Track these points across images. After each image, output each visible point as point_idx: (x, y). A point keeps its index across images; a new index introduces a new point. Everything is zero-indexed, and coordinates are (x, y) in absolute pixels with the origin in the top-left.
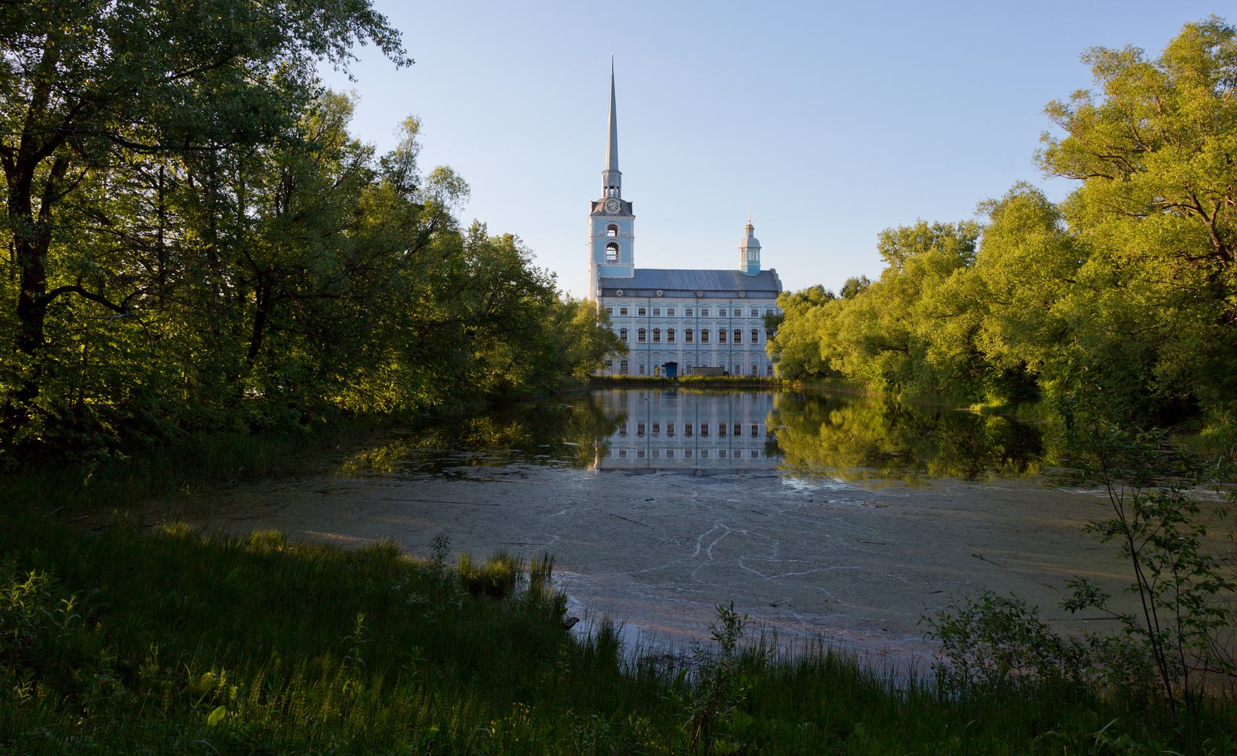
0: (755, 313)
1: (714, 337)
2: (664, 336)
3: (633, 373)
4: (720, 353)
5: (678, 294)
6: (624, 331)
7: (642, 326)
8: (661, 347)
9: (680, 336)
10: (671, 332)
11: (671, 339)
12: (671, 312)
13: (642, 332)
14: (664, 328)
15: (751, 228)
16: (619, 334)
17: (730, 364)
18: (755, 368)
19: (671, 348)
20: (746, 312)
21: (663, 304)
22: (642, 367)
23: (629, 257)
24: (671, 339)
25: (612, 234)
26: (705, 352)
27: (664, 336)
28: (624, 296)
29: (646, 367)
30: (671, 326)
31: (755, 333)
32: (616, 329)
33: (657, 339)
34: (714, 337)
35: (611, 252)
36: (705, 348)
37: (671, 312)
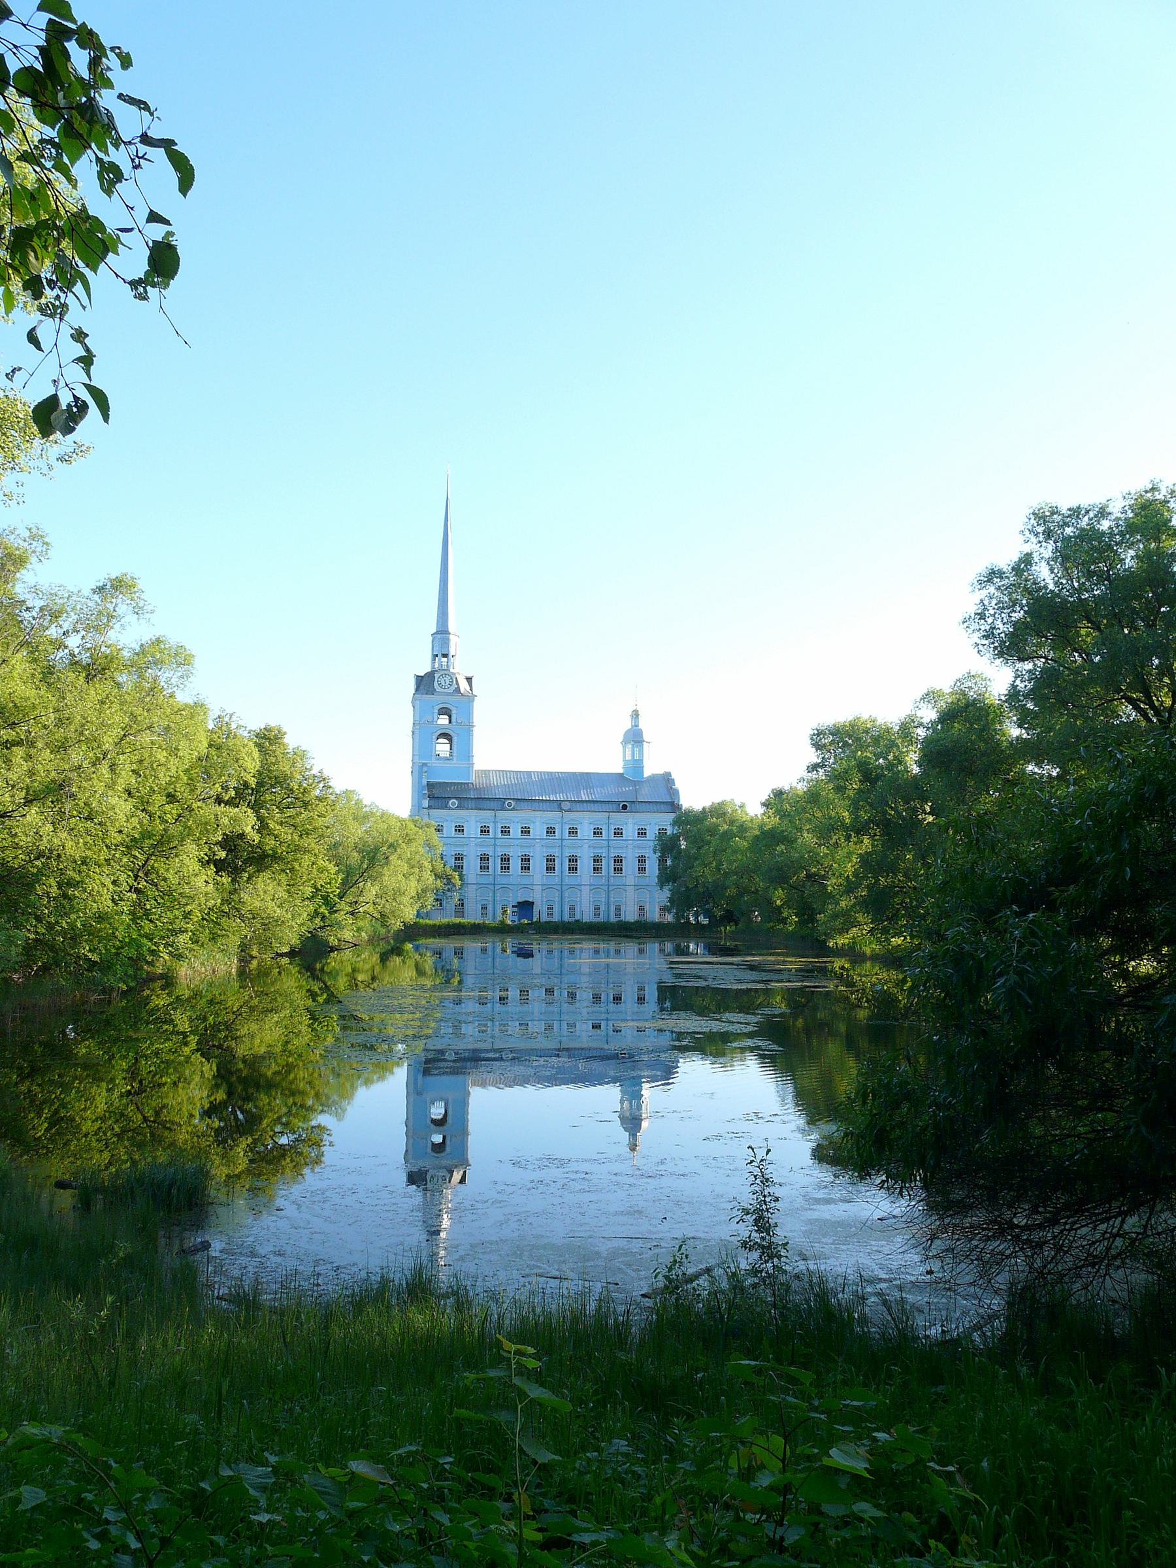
0: (642, 833)
1: (585, 865)
2: (515, 864)
4: (594, 887)
5: (535, 805)
7: (485, 850)
8: (512, 880)
9: (538, 864)
10: (526, 859)
11: (525, 868)
12: (525, 831)
13: (484, 858)
15: (636, 715)
17: (608, 904)
18: (641, 909)
19: (526, 881)
20: (630, 831)
21: (515, 819)
23: (468, 756)
24: (525, 868)
25: (443, 720)
26: (571, 886)
27: (515, 864)
28: (459, 807)
29: (490, 908)
30: (526, 851)
31: (642, 860)
33: (505, 868)
34: (585, 865)
35: (443, 748)
36: (573, 881)
37: (525, 831)
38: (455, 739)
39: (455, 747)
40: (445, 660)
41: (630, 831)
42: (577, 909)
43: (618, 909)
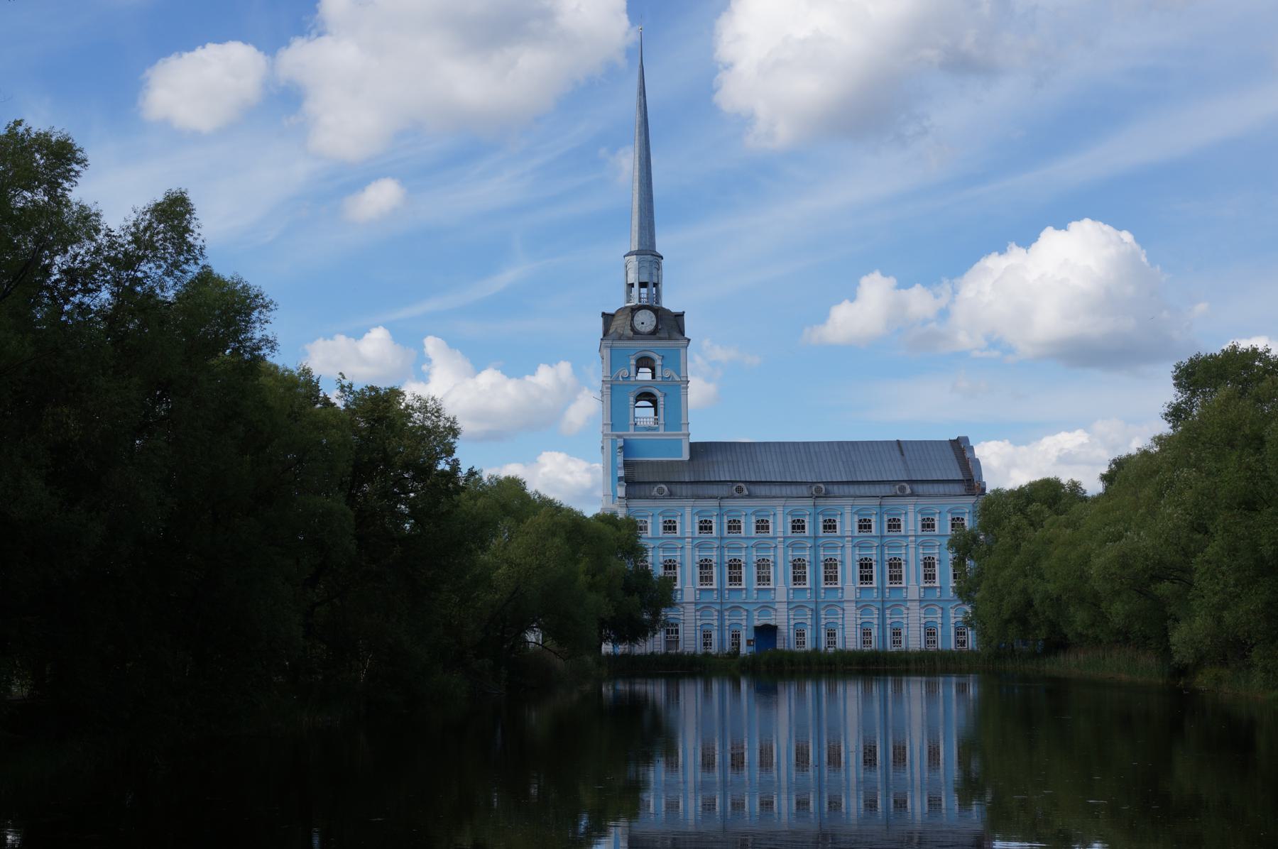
0: (928, 525)
3: (689, 642)
6: (670, 566)
11: (763, 579)
12: (762, 526)
14: (749, 558)
16: (659, 571)
20: (910, 523)
22: (707, 636)
27: (749, 575)
31: (928, 563)
32: (655, 561)
33: (735, 579)
37: (762, 526)
38: (661, 401)
39: (661, 411)
40: (644, 290)
41: (910, 523)
42: (839, 634)
43: (897, 633)
